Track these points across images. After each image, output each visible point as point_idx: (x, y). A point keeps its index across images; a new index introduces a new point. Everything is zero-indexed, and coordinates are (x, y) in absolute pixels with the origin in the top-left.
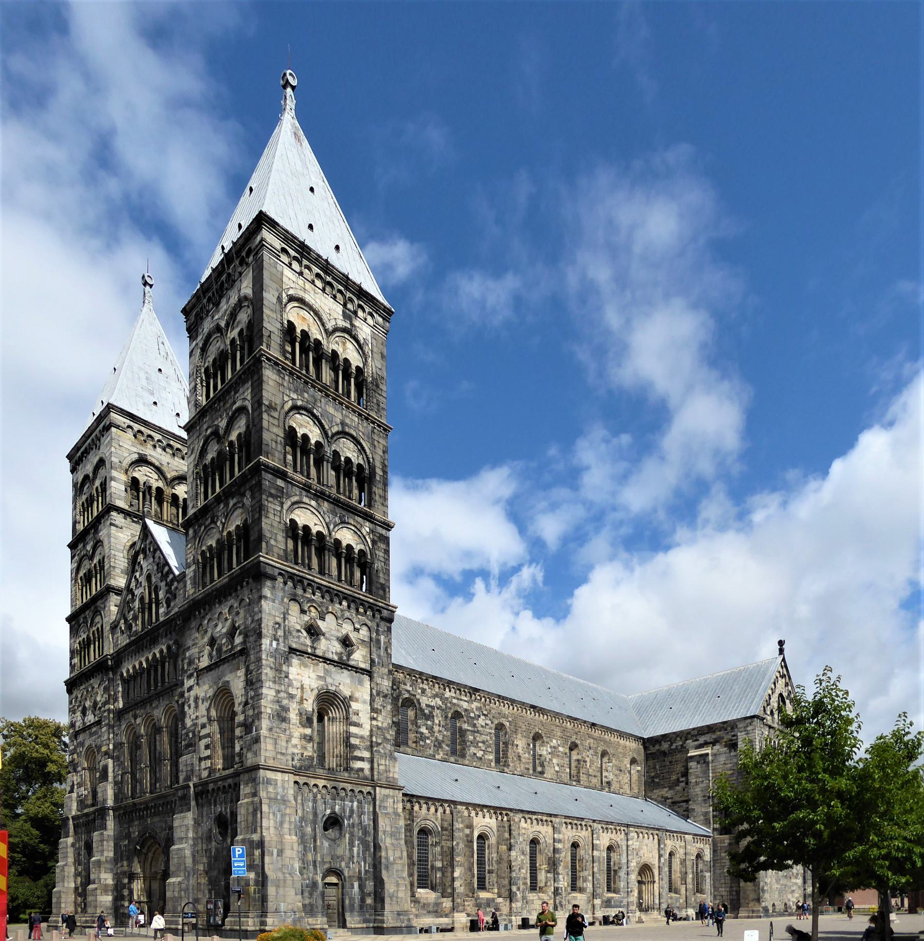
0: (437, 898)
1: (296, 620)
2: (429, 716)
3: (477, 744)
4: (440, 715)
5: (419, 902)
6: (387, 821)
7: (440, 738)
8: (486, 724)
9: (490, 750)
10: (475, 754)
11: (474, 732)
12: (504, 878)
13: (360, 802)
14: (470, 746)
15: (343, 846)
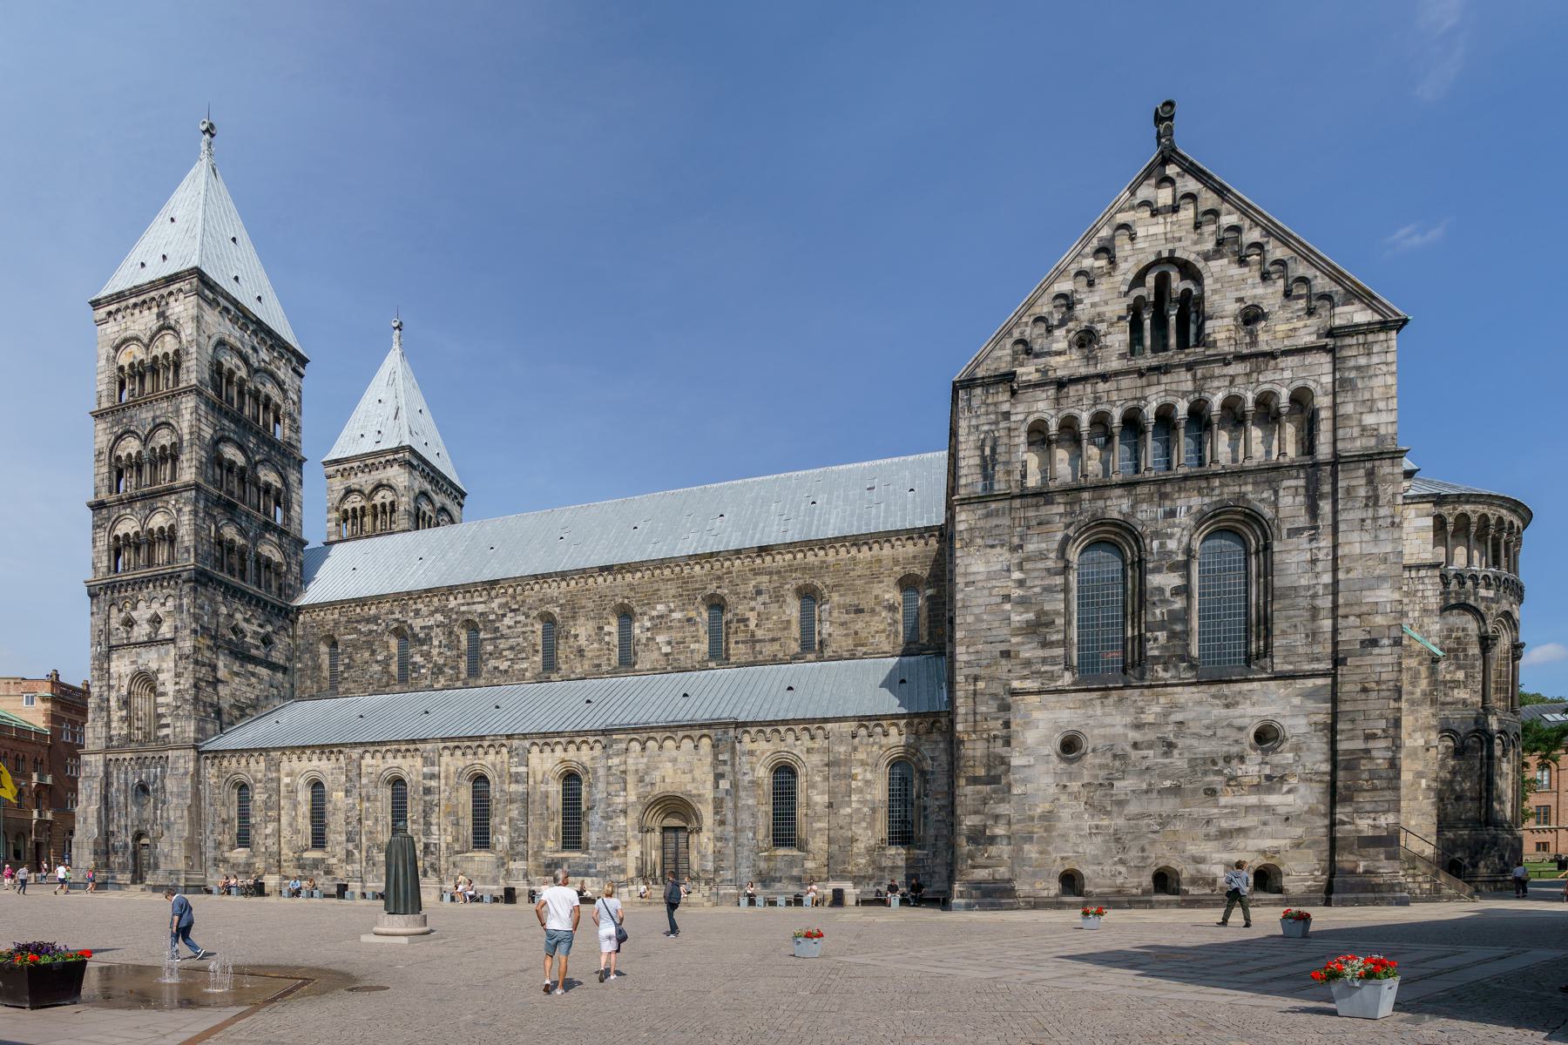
0: (249, 857)
1: (116, 619)
2: (425, 639)
3: (501, 653)
4: (441, 634)
5: (228, 862)
6: (174, 782)
7: (441, 661)
8: (516, 622)
9: (524, 655)
10: (496, 668)
11: (497, 638)
12: (339, 833)
13: (162, 767)
14: (488, 660)
15: (148, 810)
